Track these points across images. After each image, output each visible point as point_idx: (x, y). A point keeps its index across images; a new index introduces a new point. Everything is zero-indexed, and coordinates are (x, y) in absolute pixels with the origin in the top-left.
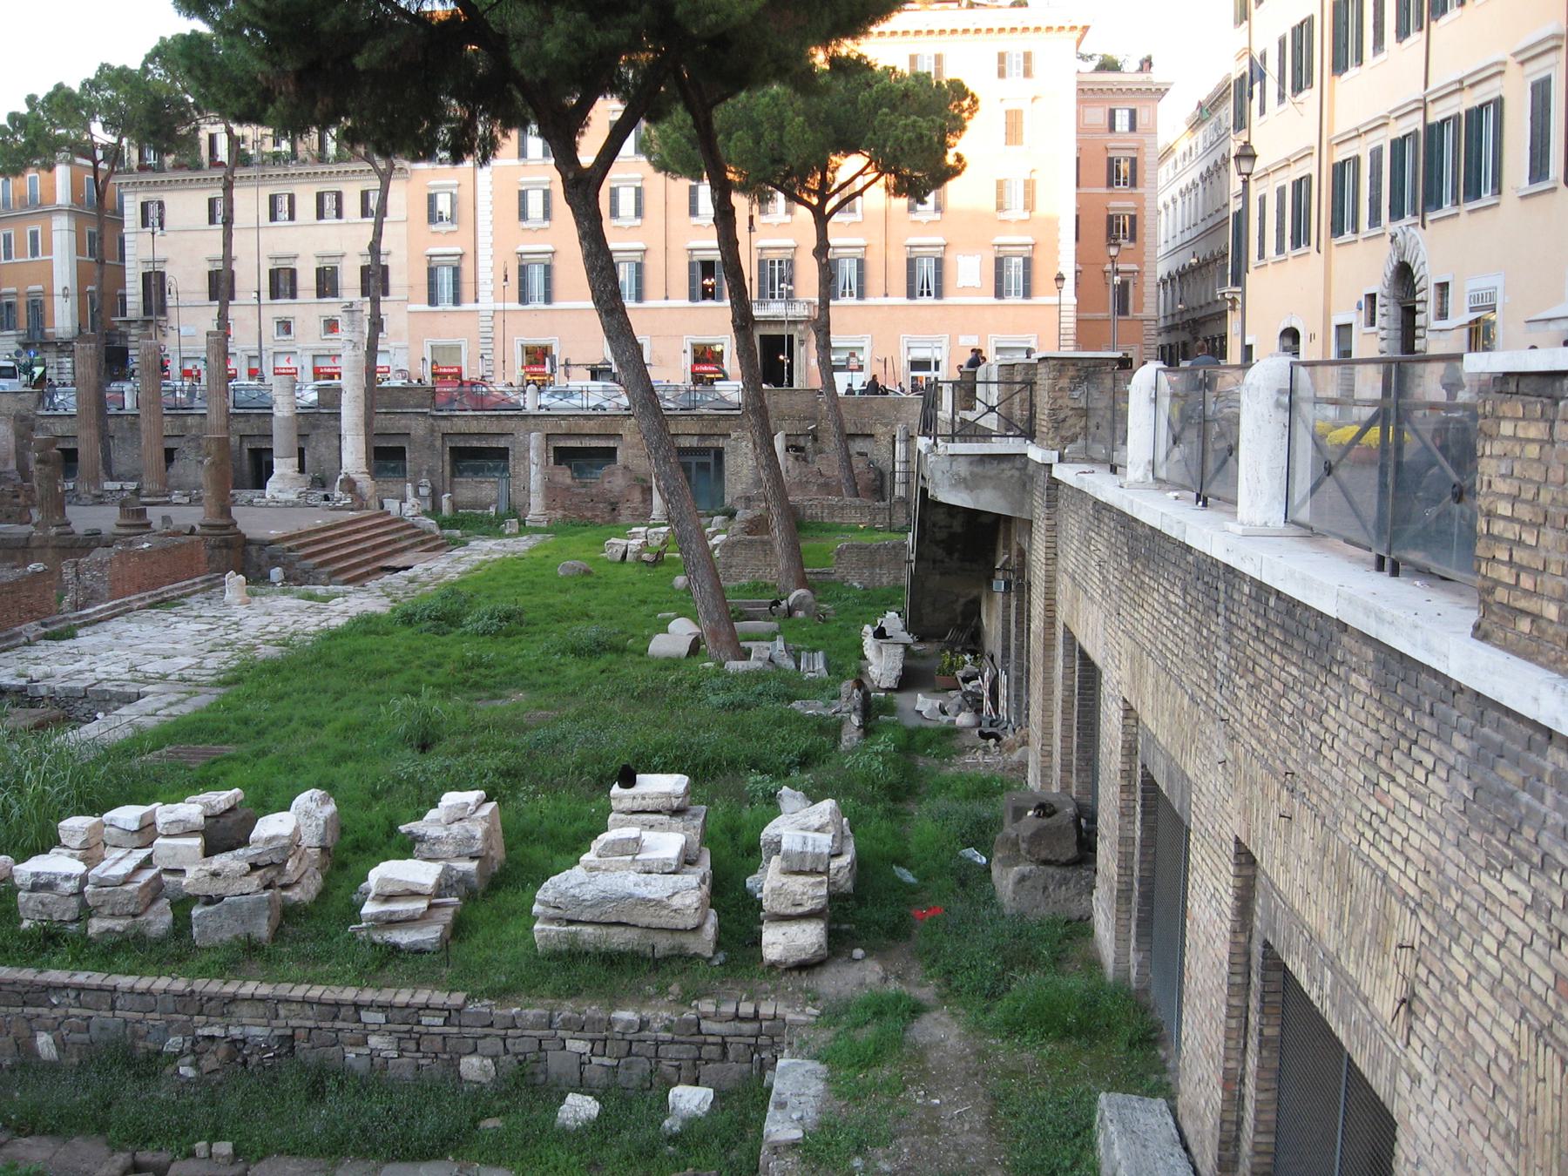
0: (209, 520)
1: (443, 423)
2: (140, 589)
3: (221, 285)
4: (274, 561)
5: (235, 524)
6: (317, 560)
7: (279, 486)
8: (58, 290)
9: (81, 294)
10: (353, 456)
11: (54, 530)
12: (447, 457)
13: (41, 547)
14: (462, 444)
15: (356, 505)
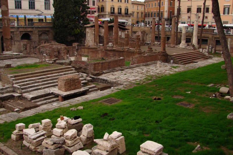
0: (161, 51)
1: (215, 36)
2: (144, 62)
3: (189, 10)
4: (172, 59)
5: (166, 52)
6: (179, 59)
7: (182, 45)
8: (165, 11)
9: (169, 12)
10: (195, 41)
11: (138, 50)
12: (215, 42)
13: (136, 53)
14: (218, 40)
15: (194, 49)
